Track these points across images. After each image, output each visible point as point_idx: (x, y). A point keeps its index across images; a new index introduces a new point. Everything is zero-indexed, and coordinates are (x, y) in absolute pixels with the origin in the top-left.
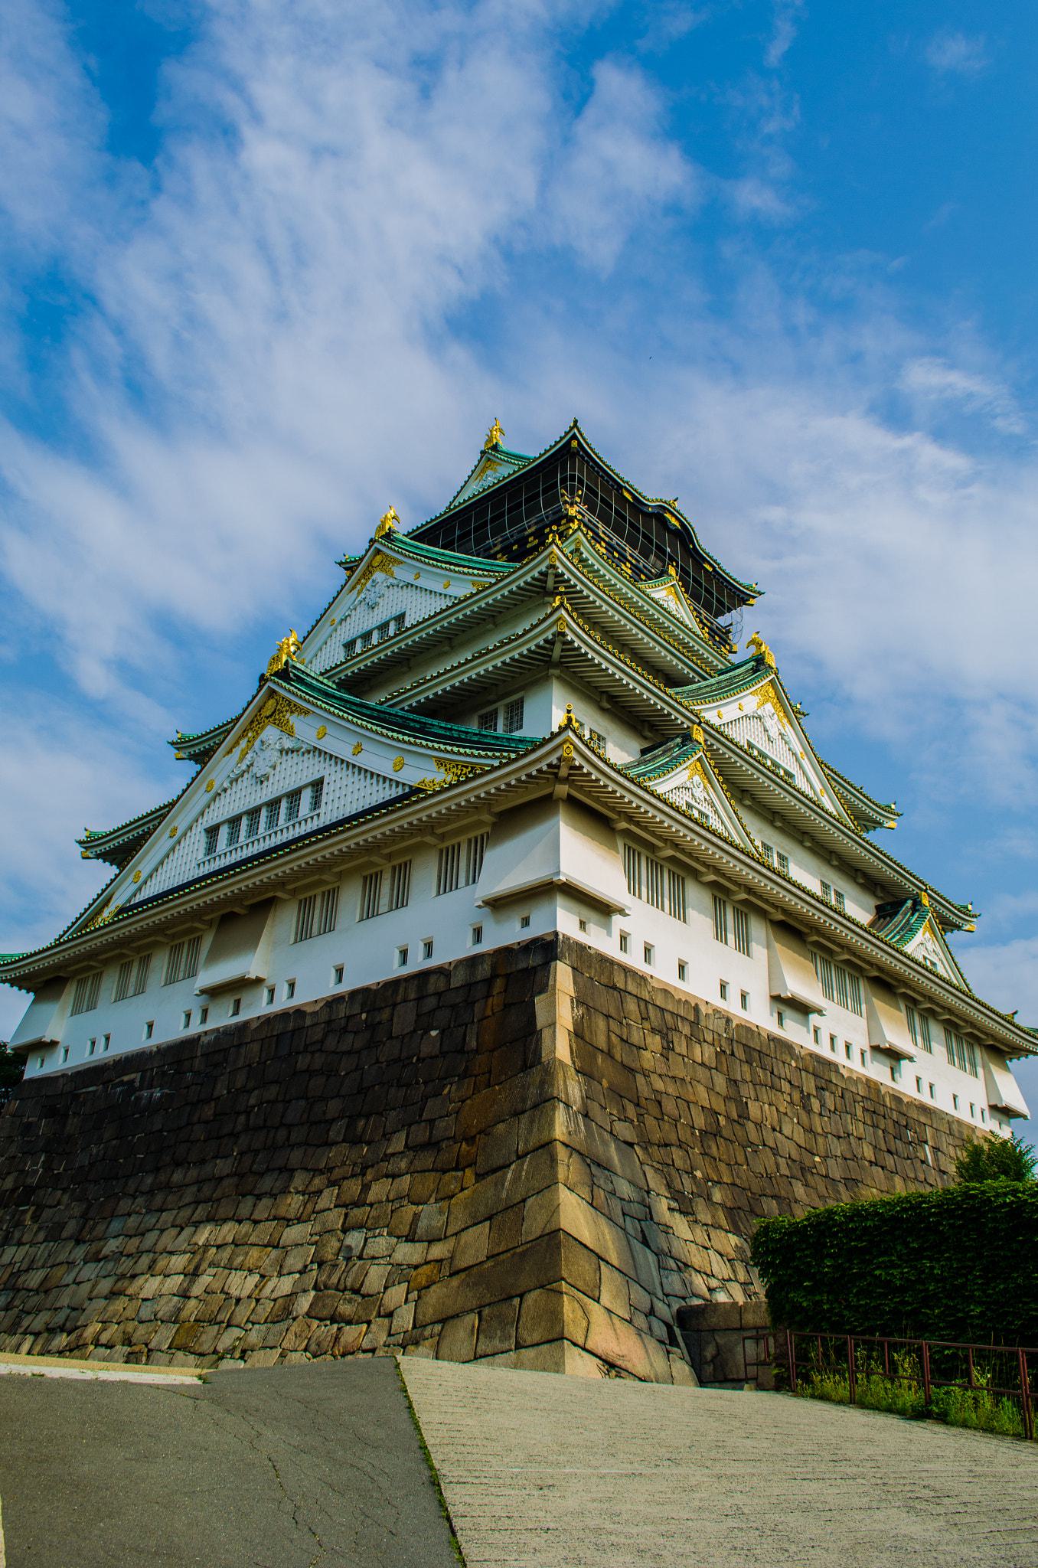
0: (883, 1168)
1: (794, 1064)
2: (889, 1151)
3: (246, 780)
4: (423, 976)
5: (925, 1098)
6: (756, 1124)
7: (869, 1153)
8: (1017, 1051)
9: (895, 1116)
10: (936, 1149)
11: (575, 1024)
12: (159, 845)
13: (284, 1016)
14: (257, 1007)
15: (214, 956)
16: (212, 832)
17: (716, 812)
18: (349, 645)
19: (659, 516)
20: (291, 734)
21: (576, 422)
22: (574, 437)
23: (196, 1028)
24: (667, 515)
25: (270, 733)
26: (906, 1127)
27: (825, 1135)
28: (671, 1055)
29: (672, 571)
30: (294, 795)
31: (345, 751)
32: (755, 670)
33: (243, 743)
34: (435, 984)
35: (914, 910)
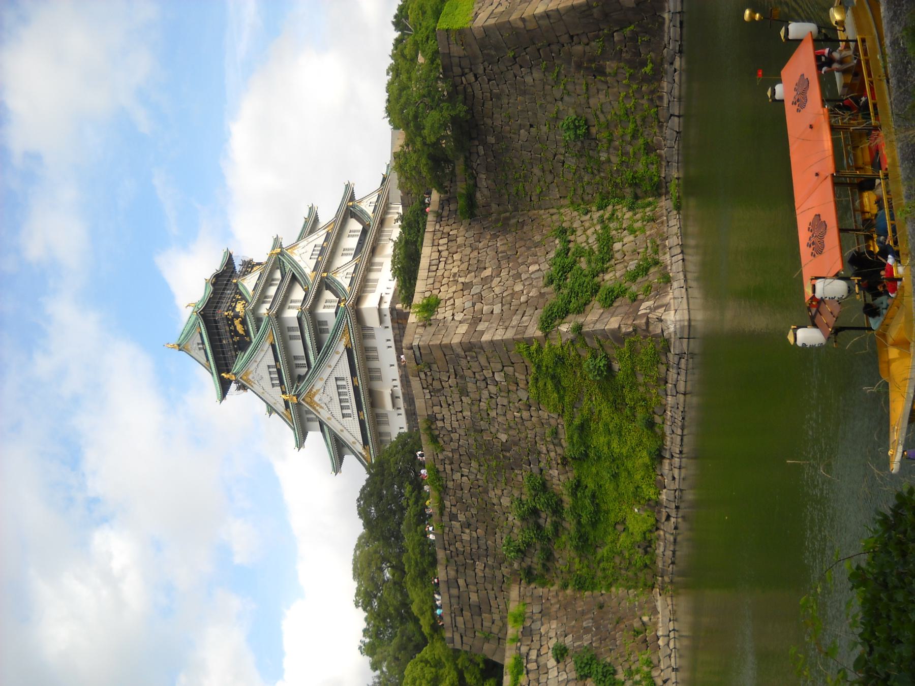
3: (330, 406)
4: (395, 341)
12: (346, 437)
13: (401, 381)
14: (399, 391)
15: (382, 406)
16: (344, 416)
18: (273, 385)
20: (318, 390)
23: (402, 411)
25: (316, 399)
29: (235, 281)
30: (338, 387)
31: (329, 370)
32: (283, 255)
33: (317, 408)
34: (398, 338)
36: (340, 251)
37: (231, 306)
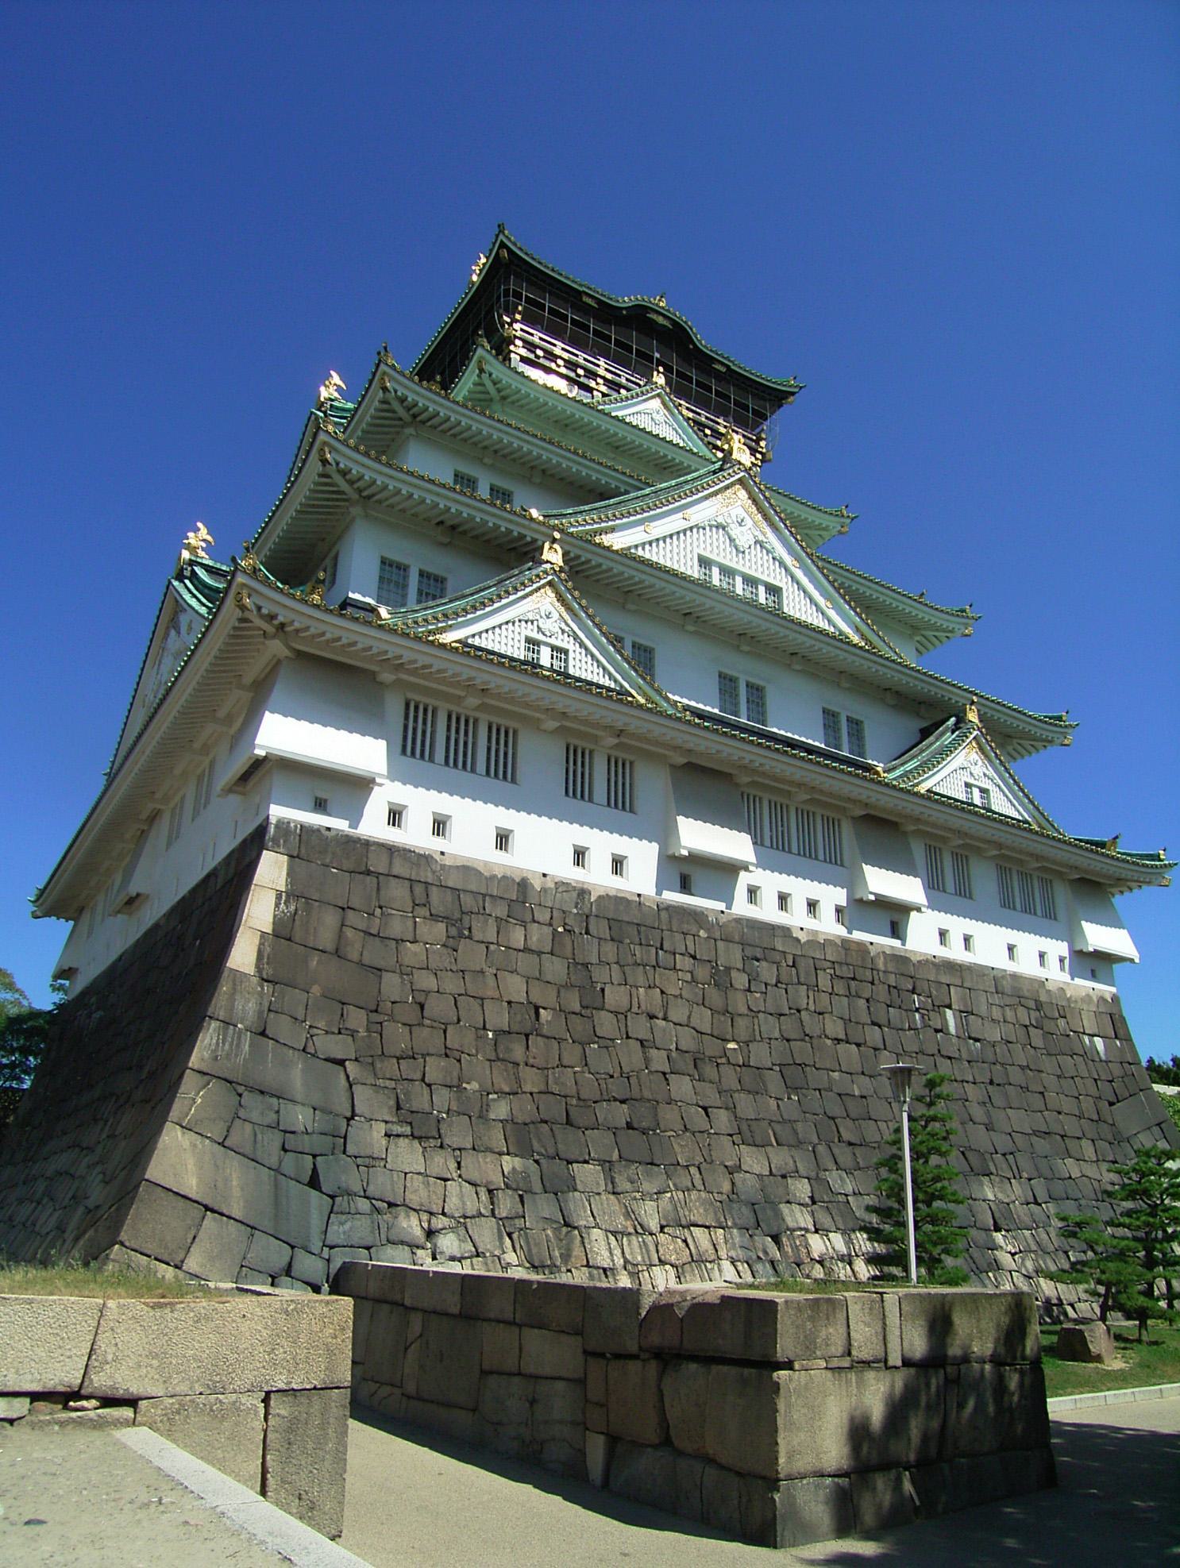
0: (858, 1045)
1: (702, 933)
2: (874, 1024)
5: (955, 952)
6: (616, 1013)
7: (835, 1028)
8: (1122, 883)
9: (892, 980)
10: (965, 1013)
11: (277, 922)
17: (582, 645)
19: (639, 318)
21: (501, 229)
22: (503, 245)
24: (654, 316)
26: (913, 992)
27: (753, 1013)
28: (463, 944)
35: (956, 727)
36: (745, 670)
37: (552, 357)
